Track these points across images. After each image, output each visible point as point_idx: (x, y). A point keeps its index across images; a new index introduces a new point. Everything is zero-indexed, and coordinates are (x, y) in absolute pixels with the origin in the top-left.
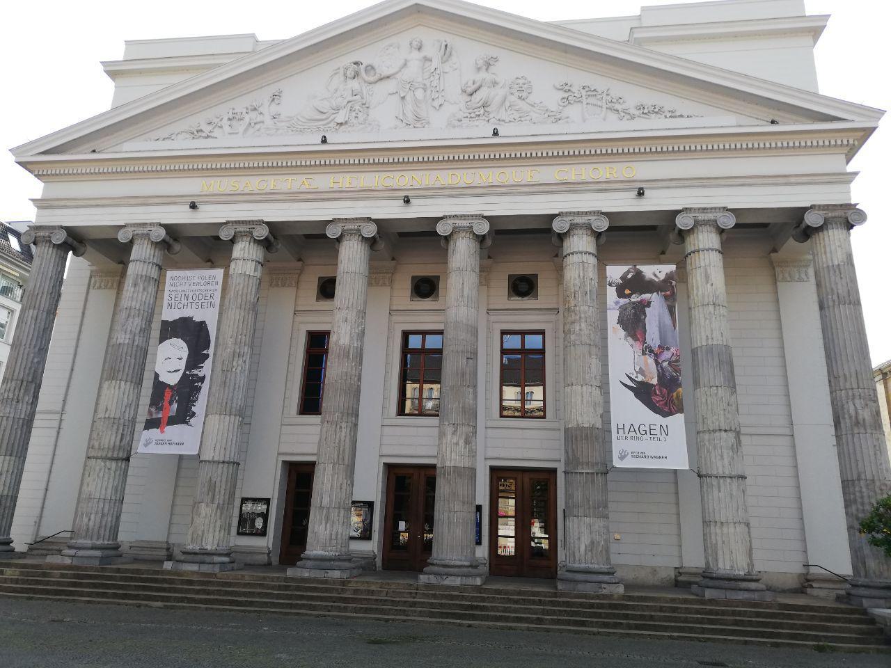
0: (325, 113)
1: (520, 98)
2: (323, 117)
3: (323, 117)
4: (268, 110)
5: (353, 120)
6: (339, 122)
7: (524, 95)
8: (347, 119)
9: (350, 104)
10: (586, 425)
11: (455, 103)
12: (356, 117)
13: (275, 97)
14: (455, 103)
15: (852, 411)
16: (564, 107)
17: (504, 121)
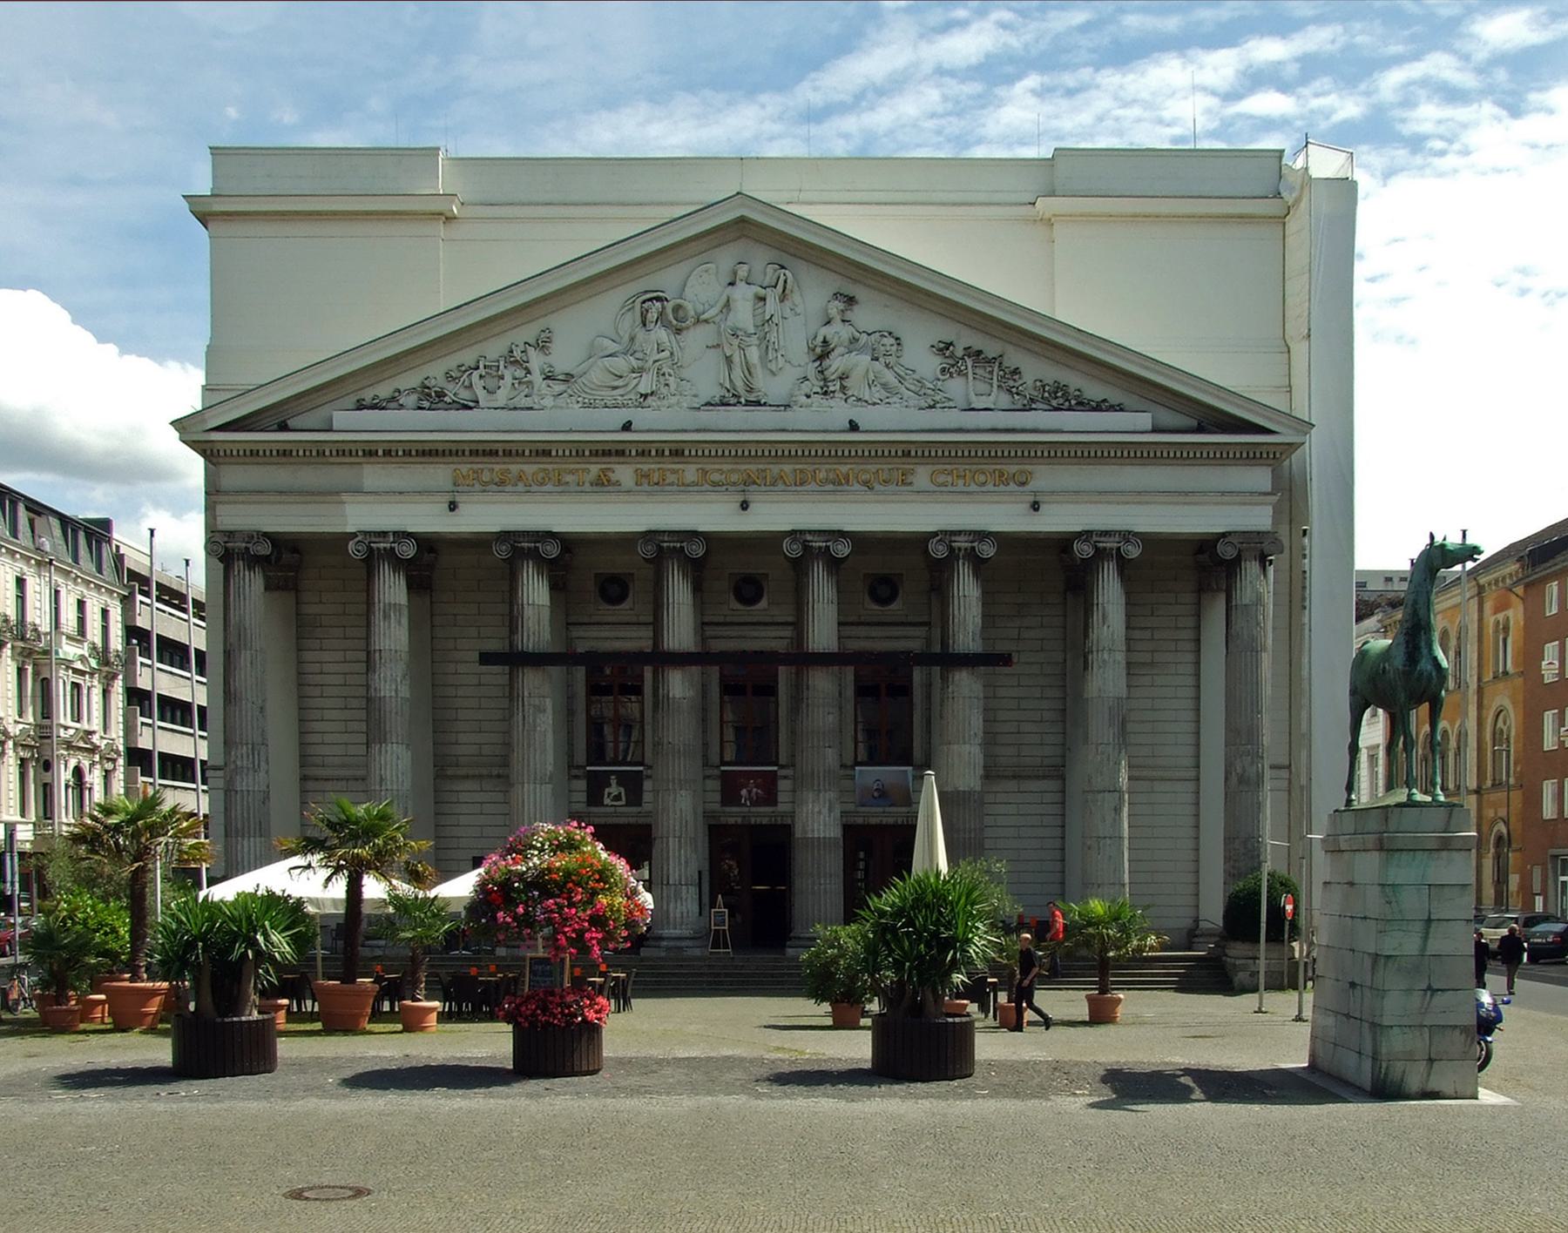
0: (621, 377)
1: (887, 366)
2: (620, 383)
3: (620, 383)
4: (536, 360)
5: (664, 390)
6: (643, 392)
7: (888, 359)
8: (654, 387)
9: (657, 364)
10: (961, 789)
11: (800, 366)
12: (667, 385)
13: (542, 345)
14: (800, 366)
15: (1239, 770)
16: (943, 381)
17: (866, 402)
